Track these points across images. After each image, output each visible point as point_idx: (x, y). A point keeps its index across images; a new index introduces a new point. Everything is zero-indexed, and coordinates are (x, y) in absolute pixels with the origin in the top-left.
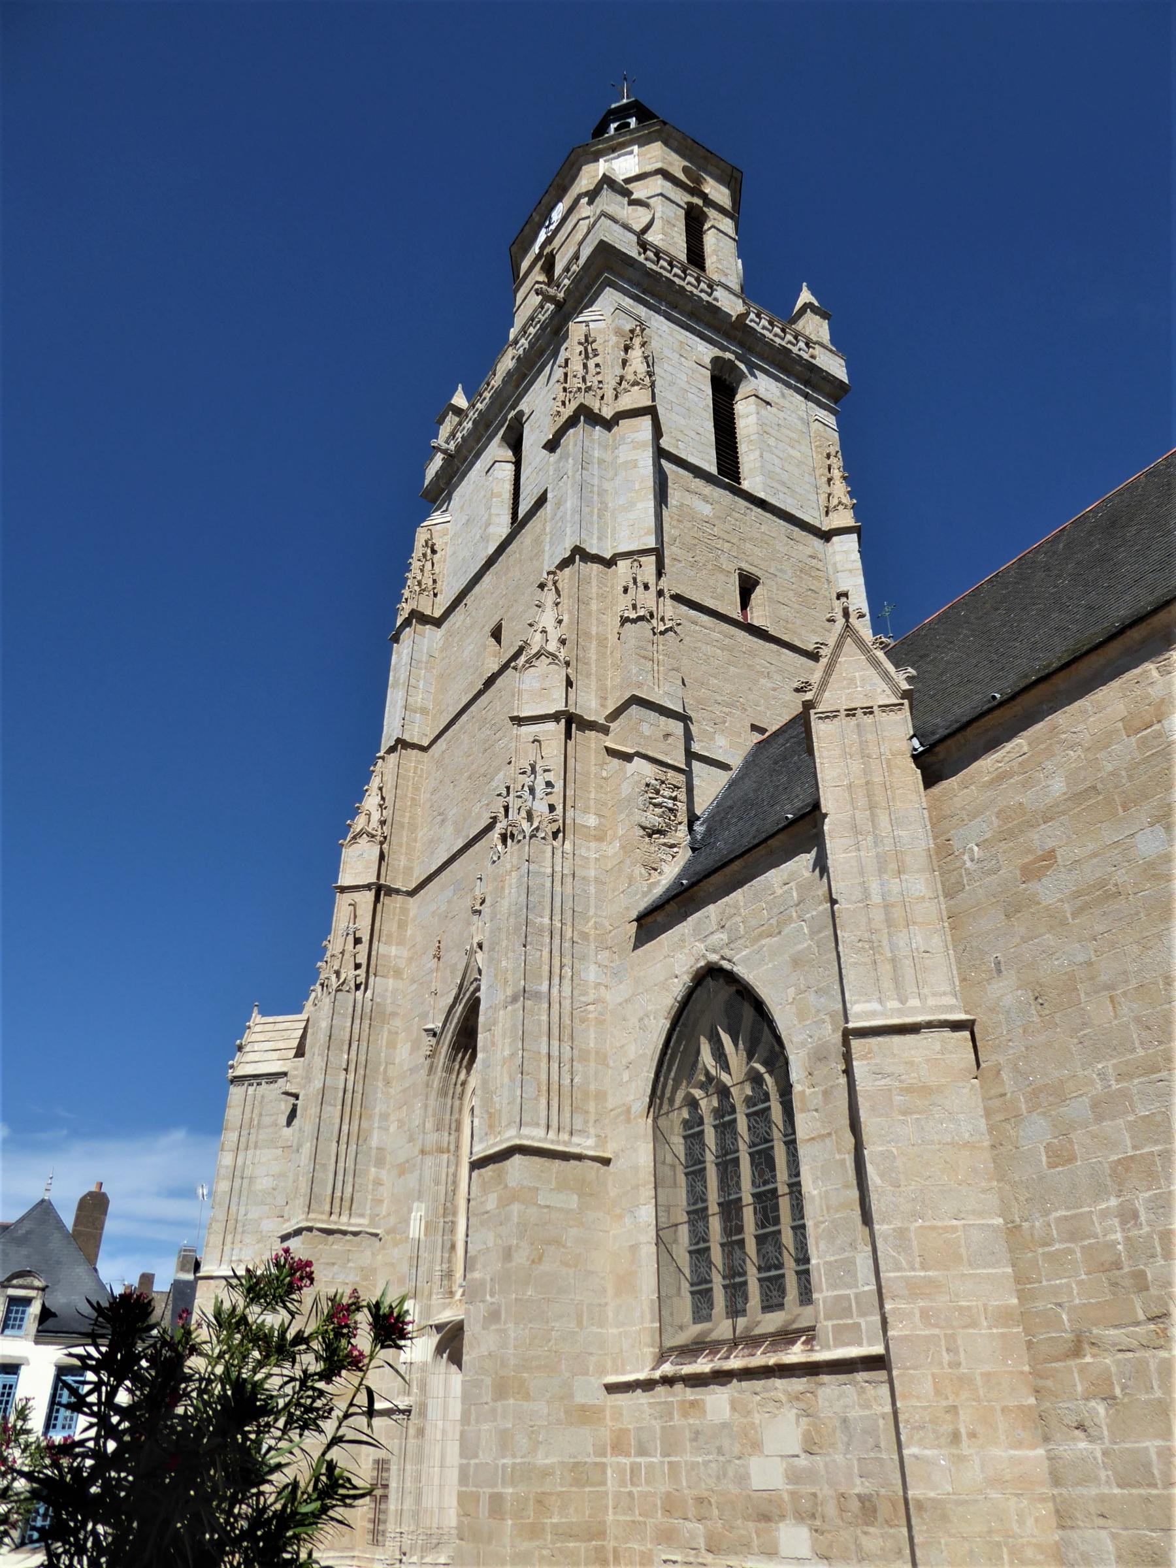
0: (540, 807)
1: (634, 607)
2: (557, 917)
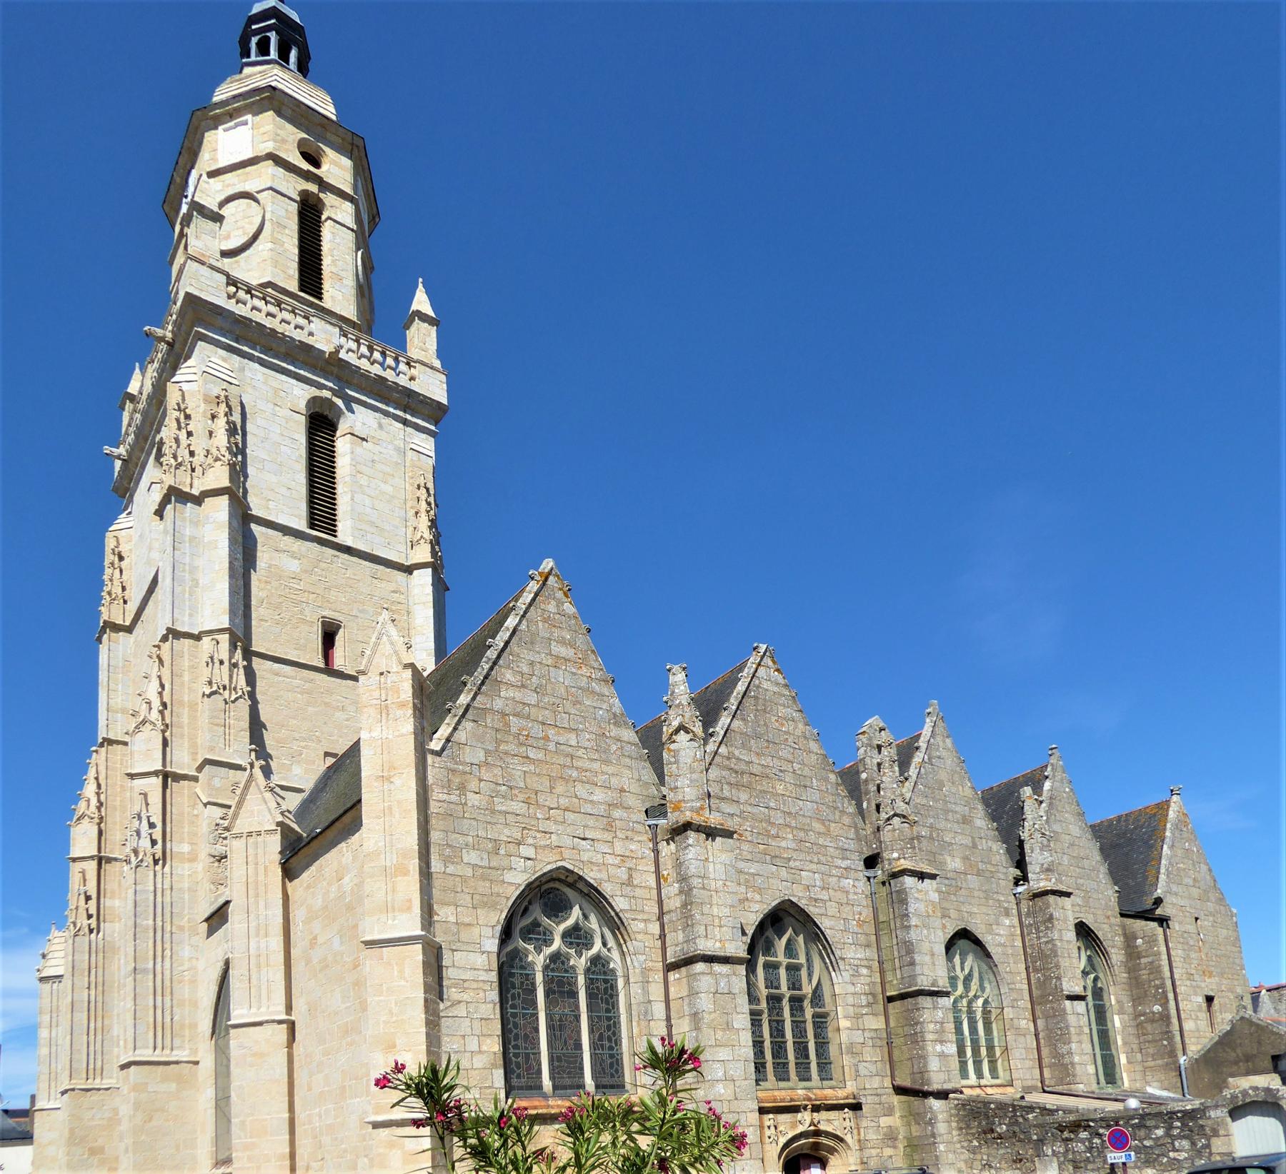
0: (145, 843)
1: (210, 683)
2: (159, 919)
